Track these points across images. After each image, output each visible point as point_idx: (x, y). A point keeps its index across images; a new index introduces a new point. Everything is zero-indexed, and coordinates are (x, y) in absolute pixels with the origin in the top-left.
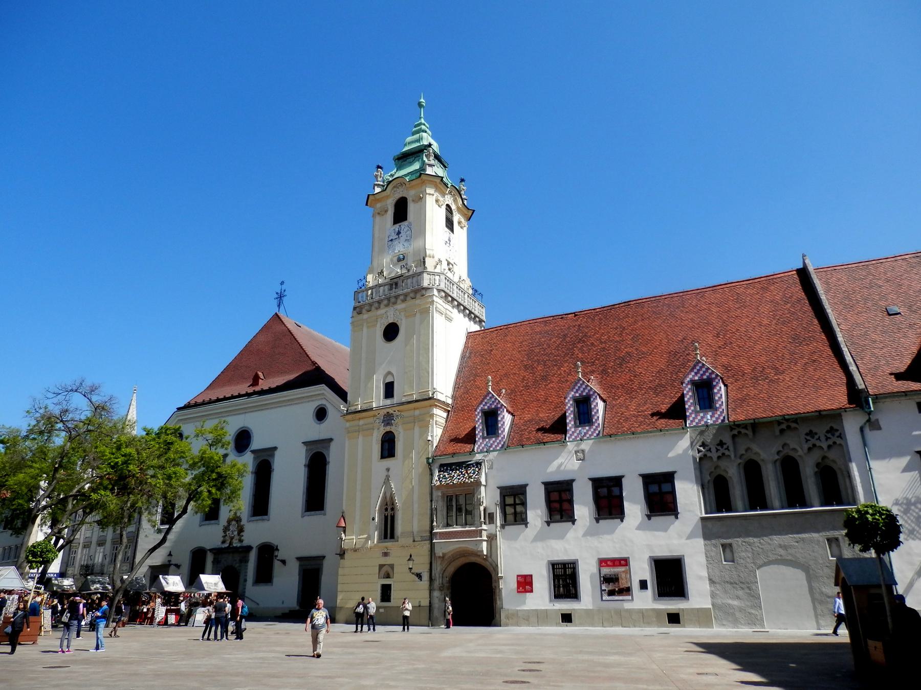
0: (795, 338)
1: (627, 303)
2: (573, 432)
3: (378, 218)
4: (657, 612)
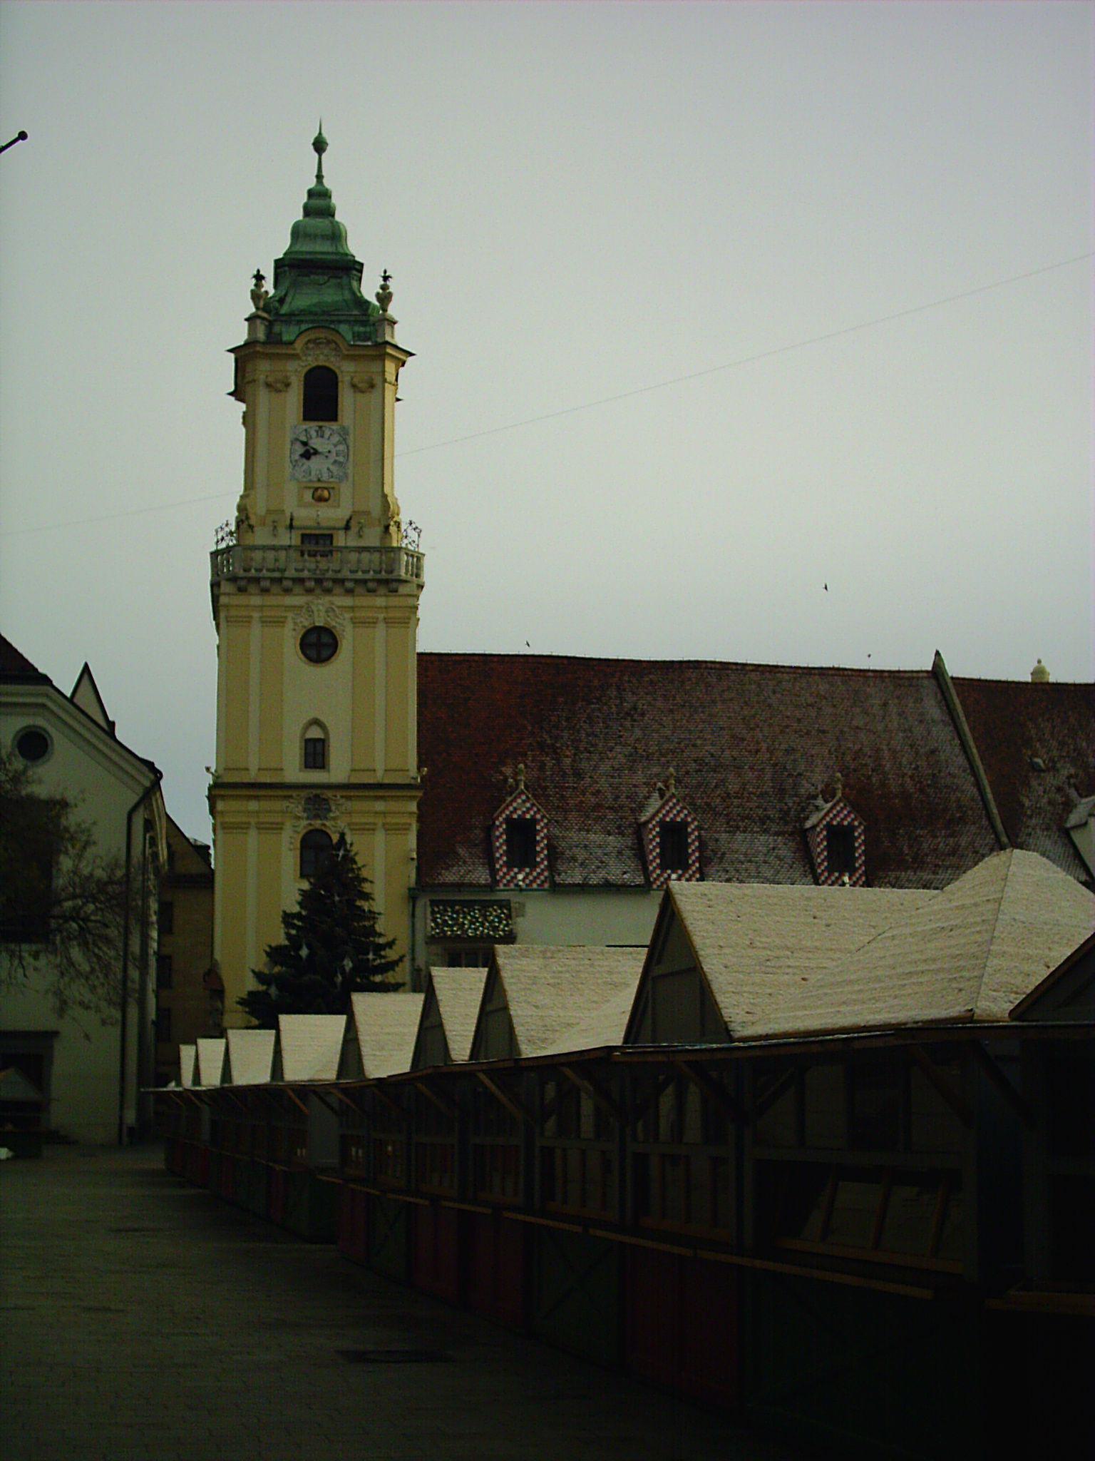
2: (659, 876)
3: (263, 396)
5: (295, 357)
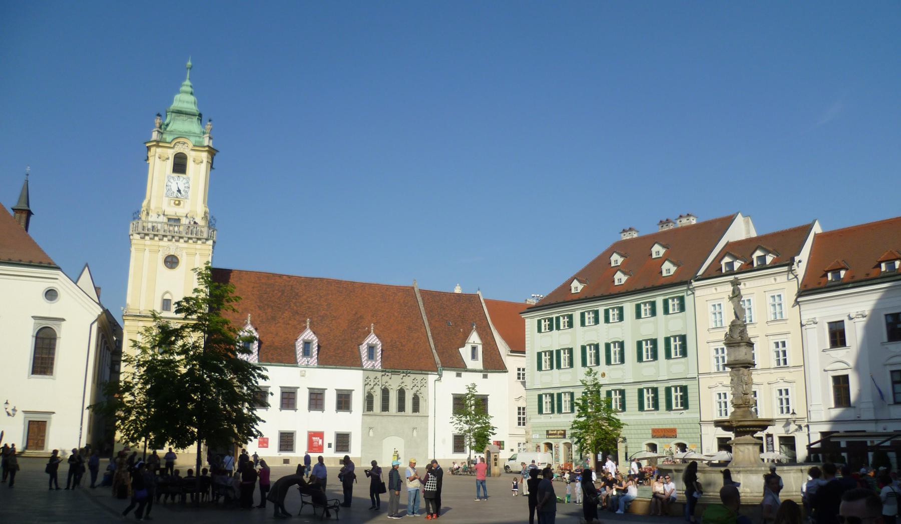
0: (410, 328)
1: (321, 279)
4: (334, 458)
5: (173, 148)
